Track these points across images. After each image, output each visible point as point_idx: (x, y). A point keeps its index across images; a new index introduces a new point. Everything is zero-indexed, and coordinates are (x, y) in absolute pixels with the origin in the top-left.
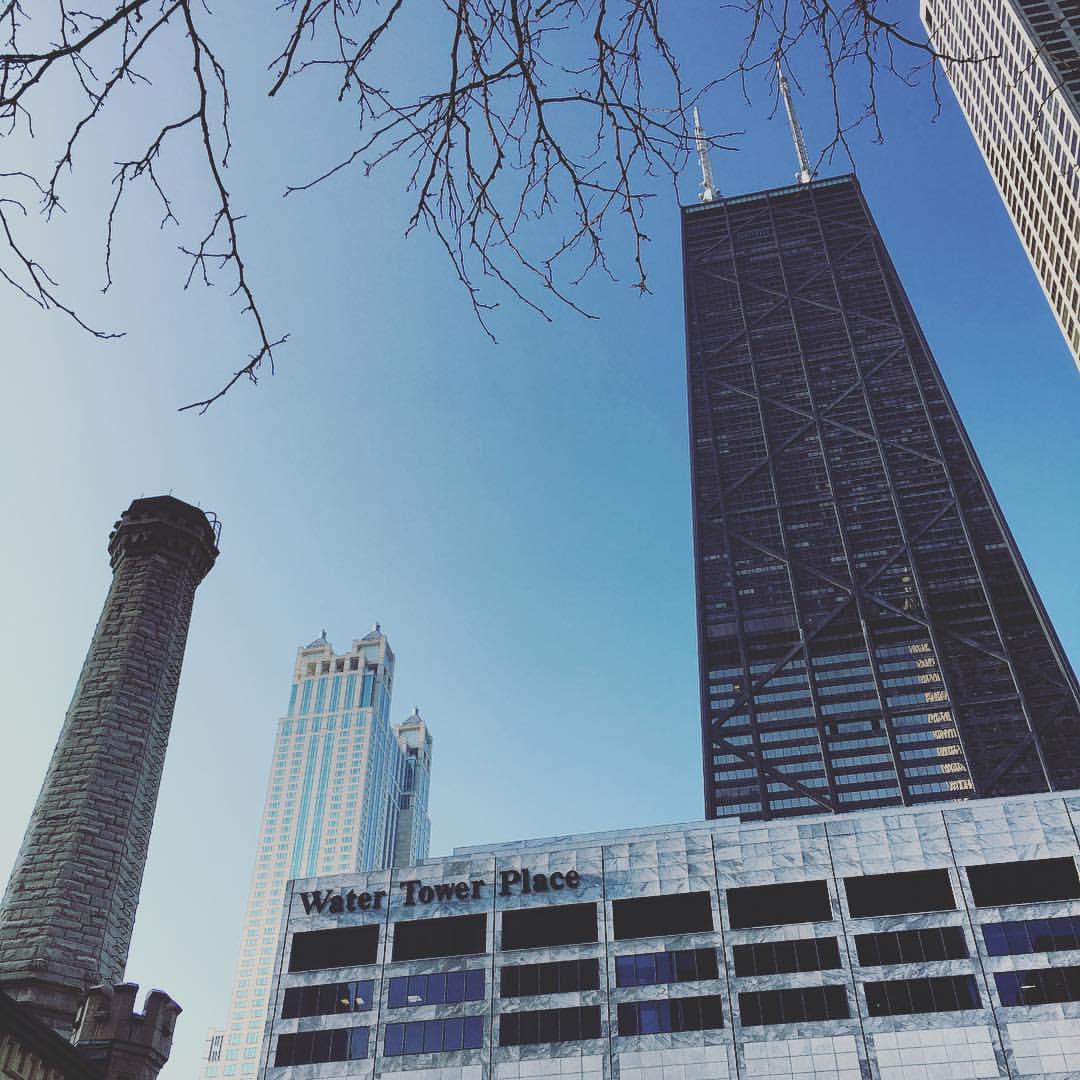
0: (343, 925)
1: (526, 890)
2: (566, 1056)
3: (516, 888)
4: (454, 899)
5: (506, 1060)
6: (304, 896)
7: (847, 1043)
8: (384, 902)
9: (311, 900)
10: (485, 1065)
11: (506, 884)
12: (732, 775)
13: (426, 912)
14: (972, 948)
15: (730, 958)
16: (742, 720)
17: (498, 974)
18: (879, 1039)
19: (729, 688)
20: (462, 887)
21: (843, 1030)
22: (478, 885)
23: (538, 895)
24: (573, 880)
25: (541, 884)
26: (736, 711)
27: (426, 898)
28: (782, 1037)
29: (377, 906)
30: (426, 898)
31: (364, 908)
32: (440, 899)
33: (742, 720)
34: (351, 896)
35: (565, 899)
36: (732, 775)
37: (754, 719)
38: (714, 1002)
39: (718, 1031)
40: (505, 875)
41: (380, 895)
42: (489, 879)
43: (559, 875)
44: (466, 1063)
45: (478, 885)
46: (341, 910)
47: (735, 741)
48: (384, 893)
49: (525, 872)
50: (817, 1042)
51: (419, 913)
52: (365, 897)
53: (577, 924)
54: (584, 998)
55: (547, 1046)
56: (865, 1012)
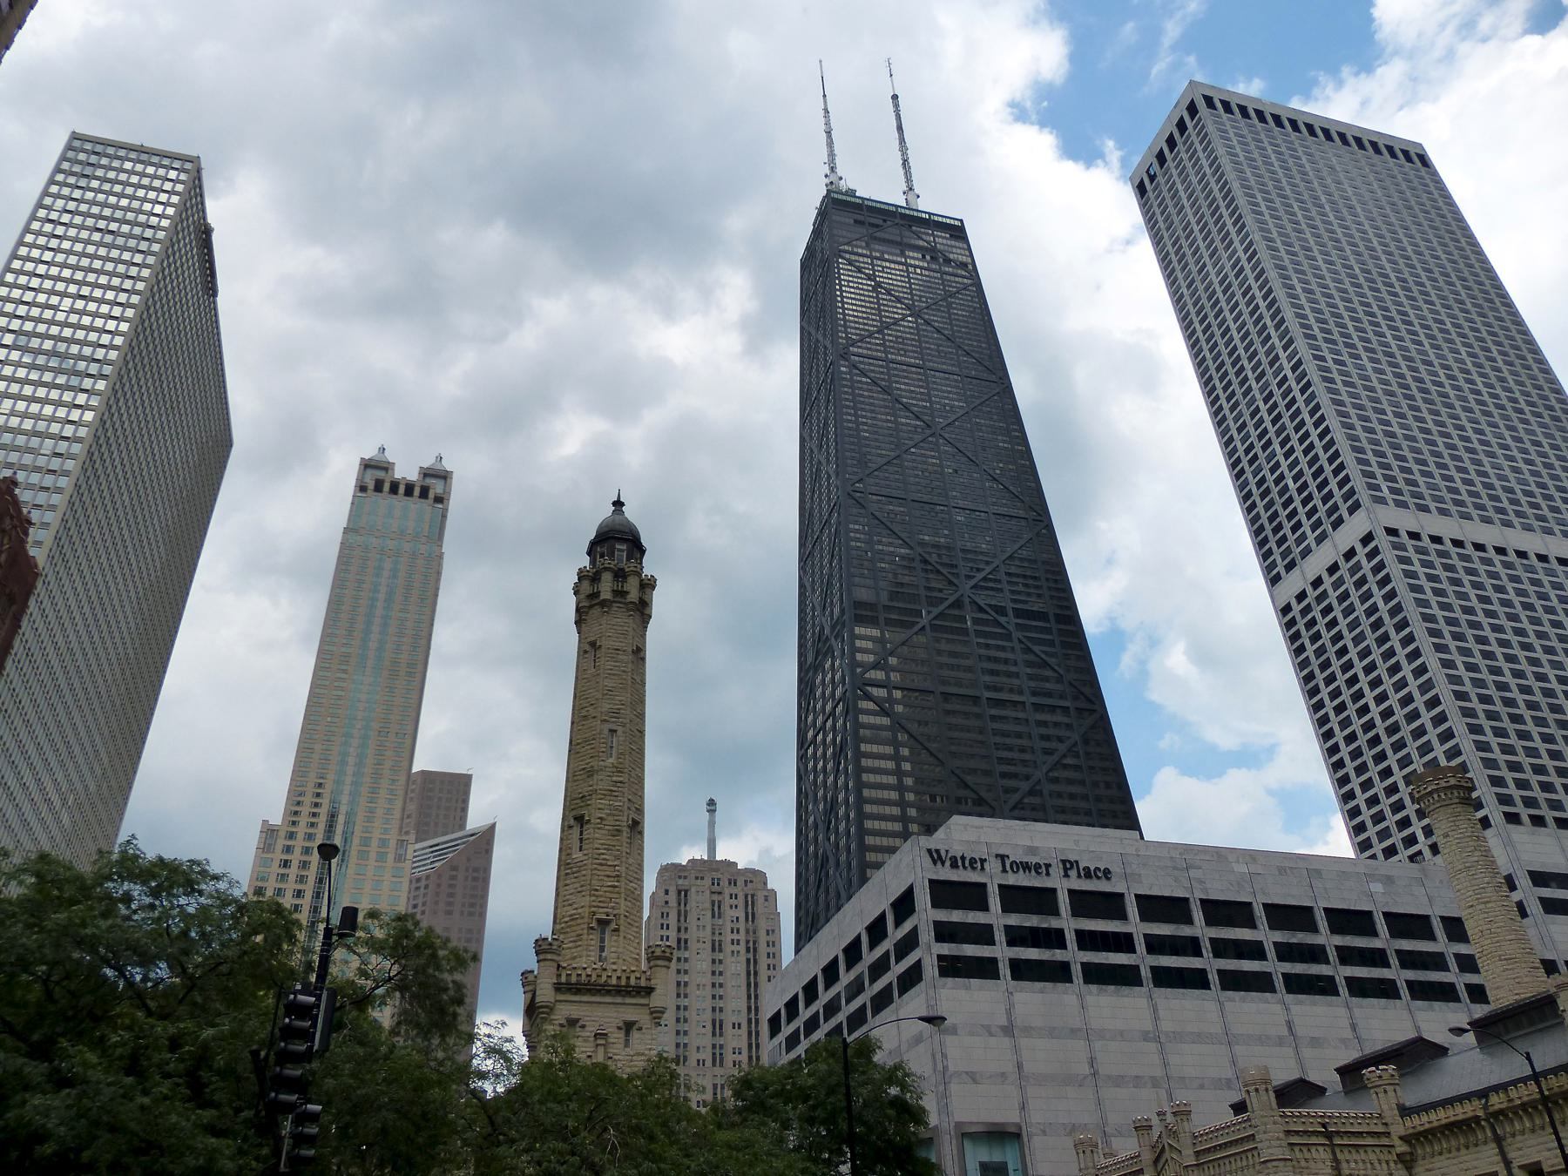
0: (961, 879)
1: (1079, 876)
3: (1073, 873)
4: (1033, 871)
5: (1090, 993)
6: (929, 851)
7: (1278, 1008)
8: (986, 866)
11: (1066, 870)
12: (872, 720)
14: (1331, 959)
15: (1208, 945)
16: (879, 675)
17: (1073, 933)
18: (1295, 1009)
19: (870, 645)
20: (1037, 866)
22: (1048, 866)
23: (1088, 881)
24: (1107, 874)
25: (1088, 874)
26: (875, 666)
29: (983, 869)
31: (974, 869)
33: (879, 675)
34: (963, 858)
36: (872, 720)
37: (888, 676)
38: (1203, 972)
40: (1064, 862)
41: (983, 861)
42: (1054, 862)
45: (1048, 866)
46: (957, 867)
47: (875, 692)
49: (1077, 862)
50: (1262, 1006)
51: (1012, 879)
52: (973, 861)
53: (1111, 905)
56: (1284, 991)
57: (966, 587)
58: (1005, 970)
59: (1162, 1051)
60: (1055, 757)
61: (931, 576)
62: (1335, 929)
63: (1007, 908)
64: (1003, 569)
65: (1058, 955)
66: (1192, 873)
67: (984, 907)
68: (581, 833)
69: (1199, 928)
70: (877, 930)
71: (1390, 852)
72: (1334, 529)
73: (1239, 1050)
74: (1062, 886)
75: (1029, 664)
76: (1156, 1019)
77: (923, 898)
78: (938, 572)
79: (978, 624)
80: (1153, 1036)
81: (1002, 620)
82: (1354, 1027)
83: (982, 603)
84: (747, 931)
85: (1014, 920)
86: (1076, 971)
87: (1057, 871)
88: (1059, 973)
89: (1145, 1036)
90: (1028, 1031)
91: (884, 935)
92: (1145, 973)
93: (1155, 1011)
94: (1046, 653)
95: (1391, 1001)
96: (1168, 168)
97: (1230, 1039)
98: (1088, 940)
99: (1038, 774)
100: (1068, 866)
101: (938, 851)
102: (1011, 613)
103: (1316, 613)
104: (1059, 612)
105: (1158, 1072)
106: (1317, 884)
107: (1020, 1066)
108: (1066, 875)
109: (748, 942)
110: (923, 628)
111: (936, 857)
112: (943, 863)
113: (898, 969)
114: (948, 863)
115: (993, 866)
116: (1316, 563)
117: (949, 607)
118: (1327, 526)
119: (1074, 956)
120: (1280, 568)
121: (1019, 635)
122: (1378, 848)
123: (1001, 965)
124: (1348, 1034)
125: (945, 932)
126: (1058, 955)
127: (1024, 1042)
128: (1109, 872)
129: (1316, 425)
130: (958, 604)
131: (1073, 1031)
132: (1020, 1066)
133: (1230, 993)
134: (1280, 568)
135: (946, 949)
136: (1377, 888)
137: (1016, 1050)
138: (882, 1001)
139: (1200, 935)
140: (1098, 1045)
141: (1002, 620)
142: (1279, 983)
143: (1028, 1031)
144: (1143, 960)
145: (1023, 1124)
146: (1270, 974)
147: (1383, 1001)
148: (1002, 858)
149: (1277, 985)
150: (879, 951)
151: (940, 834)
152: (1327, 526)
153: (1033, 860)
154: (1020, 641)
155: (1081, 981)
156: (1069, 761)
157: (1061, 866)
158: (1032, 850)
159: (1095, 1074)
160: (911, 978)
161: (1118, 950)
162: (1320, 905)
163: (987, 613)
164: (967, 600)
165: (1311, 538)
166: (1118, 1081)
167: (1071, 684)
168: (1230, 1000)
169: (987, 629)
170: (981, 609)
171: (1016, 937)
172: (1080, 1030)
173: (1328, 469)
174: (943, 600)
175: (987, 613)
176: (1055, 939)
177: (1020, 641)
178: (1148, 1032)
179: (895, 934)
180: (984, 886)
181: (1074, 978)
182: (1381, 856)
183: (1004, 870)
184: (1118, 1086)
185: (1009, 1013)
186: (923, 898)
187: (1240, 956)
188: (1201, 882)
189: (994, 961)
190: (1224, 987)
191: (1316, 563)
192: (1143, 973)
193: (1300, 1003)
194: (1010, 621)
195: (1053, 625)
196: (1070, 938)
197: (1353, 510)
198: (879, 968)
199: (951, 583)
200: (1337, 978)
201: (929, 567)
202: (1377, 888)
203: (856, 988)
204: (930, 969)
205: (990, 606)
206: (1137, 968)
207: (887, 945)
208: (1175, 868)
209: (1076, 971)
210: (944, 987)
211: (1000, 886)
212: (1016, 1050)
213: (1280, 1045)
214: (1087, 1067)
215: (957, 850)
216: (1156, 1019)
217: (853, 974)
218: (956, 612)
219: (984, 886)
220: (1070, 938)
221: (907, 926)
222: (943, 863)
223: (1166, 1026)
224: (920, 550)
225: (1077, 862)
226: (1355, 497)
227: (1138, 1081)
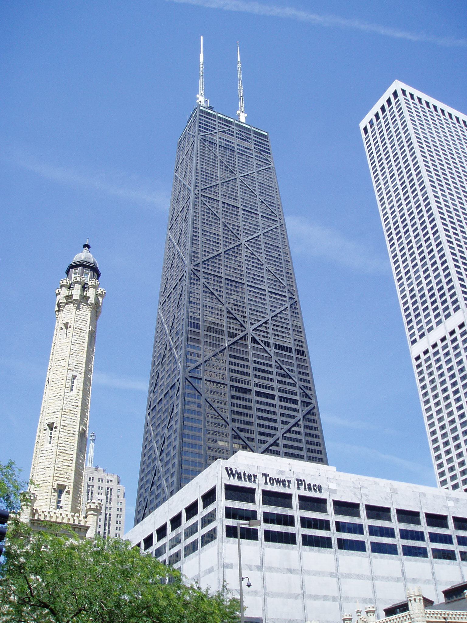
1: (305, 488)
3: (302, 487)
5: (305, 550)
6: (226, 469)
7: (398, 562)
9: (230, 472)
10: (298, 551)
11: (298, 485)
13: (272, 488)
15: (367, 529)
17: (299, 519)
20: (283, 482)
27: (272, 482)
28: (381, 558)
30: (272, 482)
32: (277, 484)
34: (244, 474)
35: (317, 495)
38: (363, 543)
39: (365, 553)
40: (297, 480)
41: (255, 476)
43: (315, 485)
44: (293, 549)
45: (289, 482)
48: (256, 475)
50: (391, 561)
51: (269, 488)
52: (249, 476)
54: (326, 533)
55: (317, 548)
57: (250, 329)
58: (261, 535)
59: (339, 583)
60: (288, 426)
61: (231, 321)
62: (430, 524)
63: (265, 503)
64: (270, 322)
65: (289, 529)
66: (364, 491)
67: (253, 501)
68: (51, 433)
69: (364, 520)
70: (192, 510)
71: (455, 487)
72: (446, 319)
73: (377, 583)
74: (295, 492)
75: (278, 374)
76: (337, 565)
77: (220, 494)
78: (236, 319)
79: (254, 350)
80: (335, 575)
81: (266, 348)
82: (433, 574)
83: (257, 338)
84: (106, 508)
85: (269, 509)
86: (299, 539)
87: (294, 484)
88: (289, 539)
89: (331, 575)
90: (271, 569)
91: (196, 513)
92: (334, 542)
93: (337, 561)
94: (289, 370)
95: (452, 561)
96: (380, 122)
97: (373, 578)
98: (306, 523)
99: (279, 434)
100: (300, 482)
101: (231, 469)
102: (272, 345)
103: (432, 361)
104: (298, 348)
105: (336, 594)
106: (424, 501)
107: (264, 587)
108: (298, 488)
109: (106, 514)
110: (224, 349)
111: (230, 473)
112: (234, 476)
113: (203, 531)
115: (261, 480)
116: (435, 336)
117: (240, 339)
118: (442, 317)
119: (298, 530)
120: (417, 336)
121: (276, 358)
122: (450, 484)
124: (430, 577)
125: (231, 513)
126: (289, 529)
127: (267, 574)
128: (320, 486)
129: (442, 264)
130: (244, 338)
132: (264, 587)
133: (376, 554)
134: (417, 336)
135: (231, 522)
136: (451, 504)
137: (263, 578)
138: (192, 548)
139: (363, 524)
140: (306, 577)
141: (266, 348)
142: (400, 550)
143: (271, 569)
144: (334, 535)
145: (264, 619)
146: (396, 545)
147: (448, 561)
148: (266, 475)
149: (398, 550)
150: (192, 521)
151: (232, 459)
152: (442, 317)
153: (281, 478)
154: (276, 362)
155: (301, 544)
156: (295, 429)
157: (296, 482)
158: (281, 472)
159: (303, 593)
160: (210, 537)
161: (321, 528)
162: (423, 510)
163: (260, 344)
164: (249, 337)
165: (434, 322)
166: (316, 597)
167: (300, 388)
168: (375, 557)
169: (259, 353)
170: (257, 342)
171: (269, 518)
172: (298, 570)
173: (446, 288)
174: (237, 335)
175: (260, 344)
176: (288, 521)
177: (276, 362)
178: (333, 573)
179: (202, 512)
181: (297, 542)
182: (451, 488)
183: (266, 483)
184: (315, 600)
185: (262, 559)
186: (220, 494)
187: (382, 535)
188: (367, 495)
190: (374, 551)
191: (435, 336)
192: (333, 542)
193: (410, 560)
194: (272, 350)
195: (294, 354)
196: (297, 521)
197: (456, 310)
198: (192, 530)
199: (242, 326)
200: (428, 548)
201: (231, 316)
202: (451, 504)
203: (177, 541)
204: (221, 532)
205: (262, 341)
206: (329, 539)
207: (197, 518)
208: (354, 488)
209: (299, 539)
210: (228, 542)
211: (263, 491)
212: (263, 578)
213: (398, 581)
214: (300, 589)
215: (241, 470)
216: (337, 565)
217: (174, 534)
218: (244, 342)
220: (297, 521)
221: (210, 509)
222: (234, 476)
223: (342, 570)
224: (227, 305)
225: (304, 481)
226: (457, 304)
227: (325, 598)
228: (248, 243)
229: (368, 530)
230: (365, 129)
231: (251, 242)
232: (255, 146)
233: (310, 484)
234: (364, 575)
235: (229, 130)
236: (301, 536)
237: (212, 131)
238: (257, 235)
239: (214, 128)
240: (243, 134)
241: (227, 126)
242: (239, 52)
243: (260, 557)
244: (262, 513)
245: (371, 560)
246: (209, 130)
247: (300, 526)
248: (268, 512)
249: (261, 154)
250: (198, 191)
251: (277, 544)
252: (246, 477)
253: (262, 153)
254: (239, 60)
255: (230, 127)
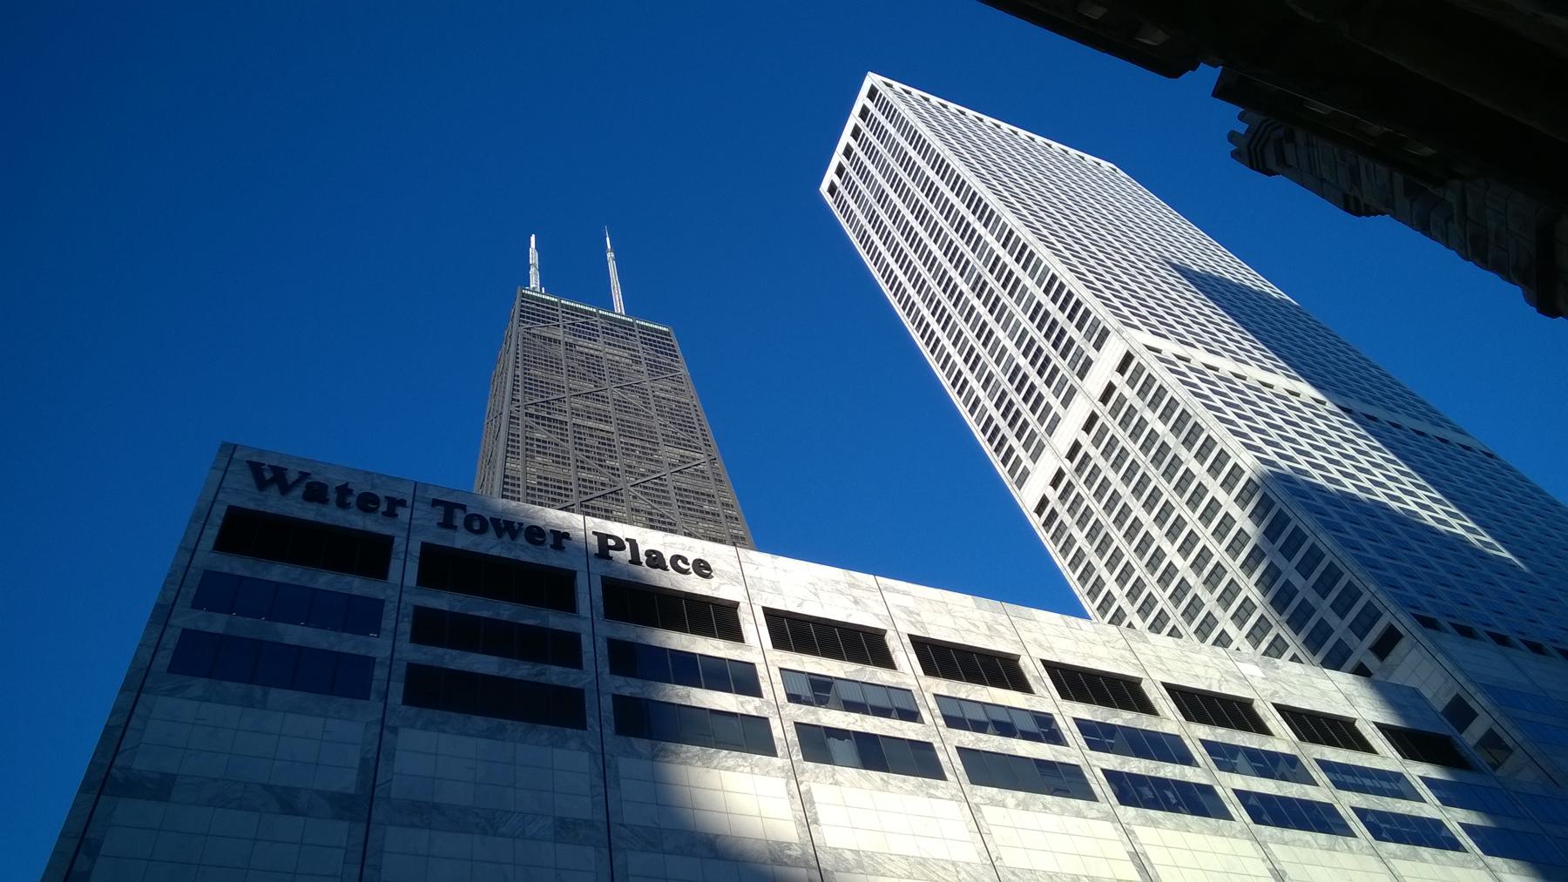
2: (728, 769)
7: (1107, 828)
8: (403, 514)
21: (1094, 814)
27: (476, 526)
30: (476, 526)
32: (499, 536)
39: (941, 783)
48: (403, 503)
50: (1071, 822)
86: (600, 709)
90: (424, 813)
114: (299, 491)
118: (1073, 380)
123: (380, 673)
131: (565, 829)
180: (388, 541)
181: (590, 720)
183: (447, 524)
189: (366, 663)
193: (1155, 823)
211: (426, 548)
219: (388, 541)
228: (639, 488)
229: (937, 712)
230: (832, 189)
231: (645, 487)
232: (644, 346)
233: (659, 555)
234: (954, 864)
235: (587, 323)
236: (607, 703)
237: (549, 323)
238: (658, 475)
239: (554, 319)
240: (617, 328)
241: (582, 317)
242: (608, 239)
243: (364, 760)
244: (410, 610)
245: (974, 811)
246: (544, 322)
247: (607, 670)
248: (446, 608)
249: (658, 357)
250: (518, 407)
251: (478, 719)
252: (352, 500)
253: (659, 355)
254: (609, 247)
255: (587, 318)
